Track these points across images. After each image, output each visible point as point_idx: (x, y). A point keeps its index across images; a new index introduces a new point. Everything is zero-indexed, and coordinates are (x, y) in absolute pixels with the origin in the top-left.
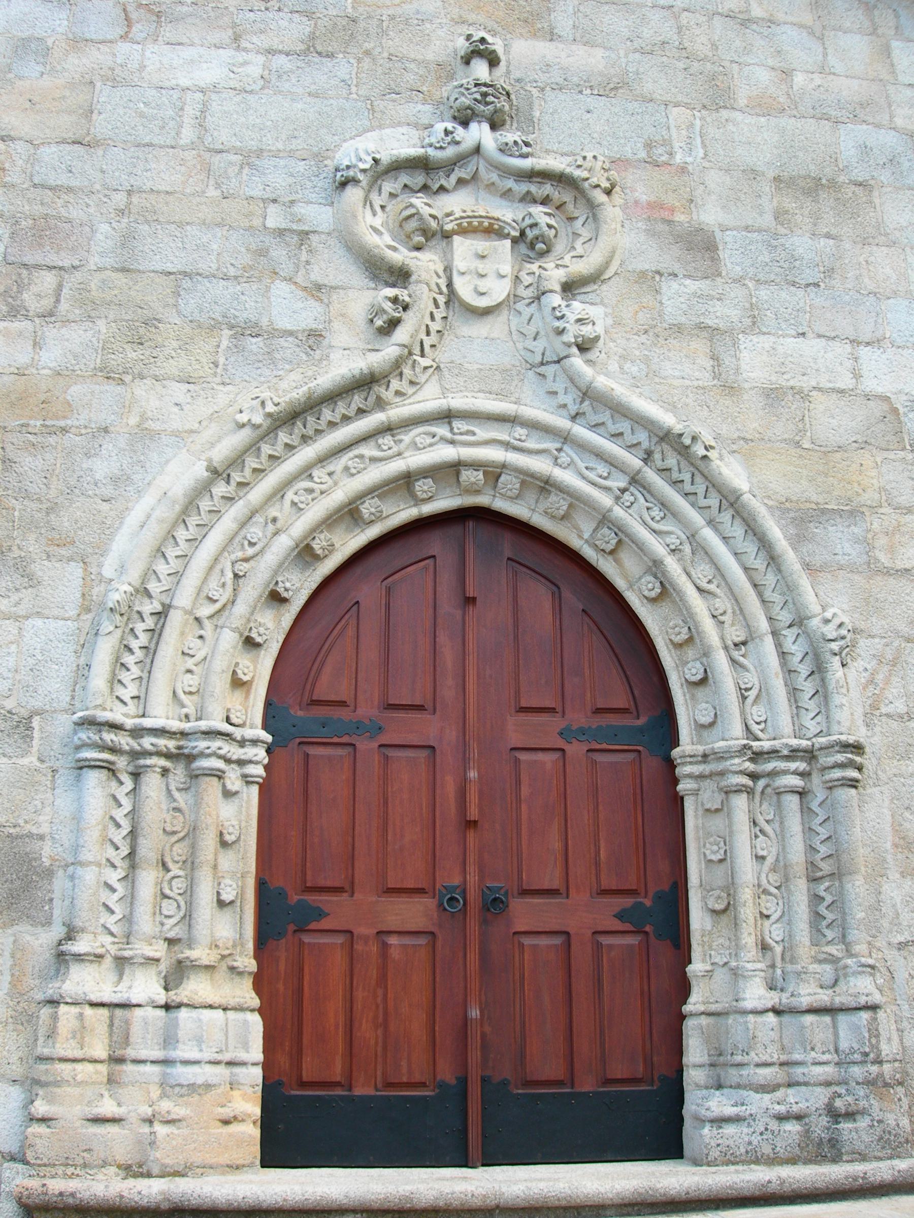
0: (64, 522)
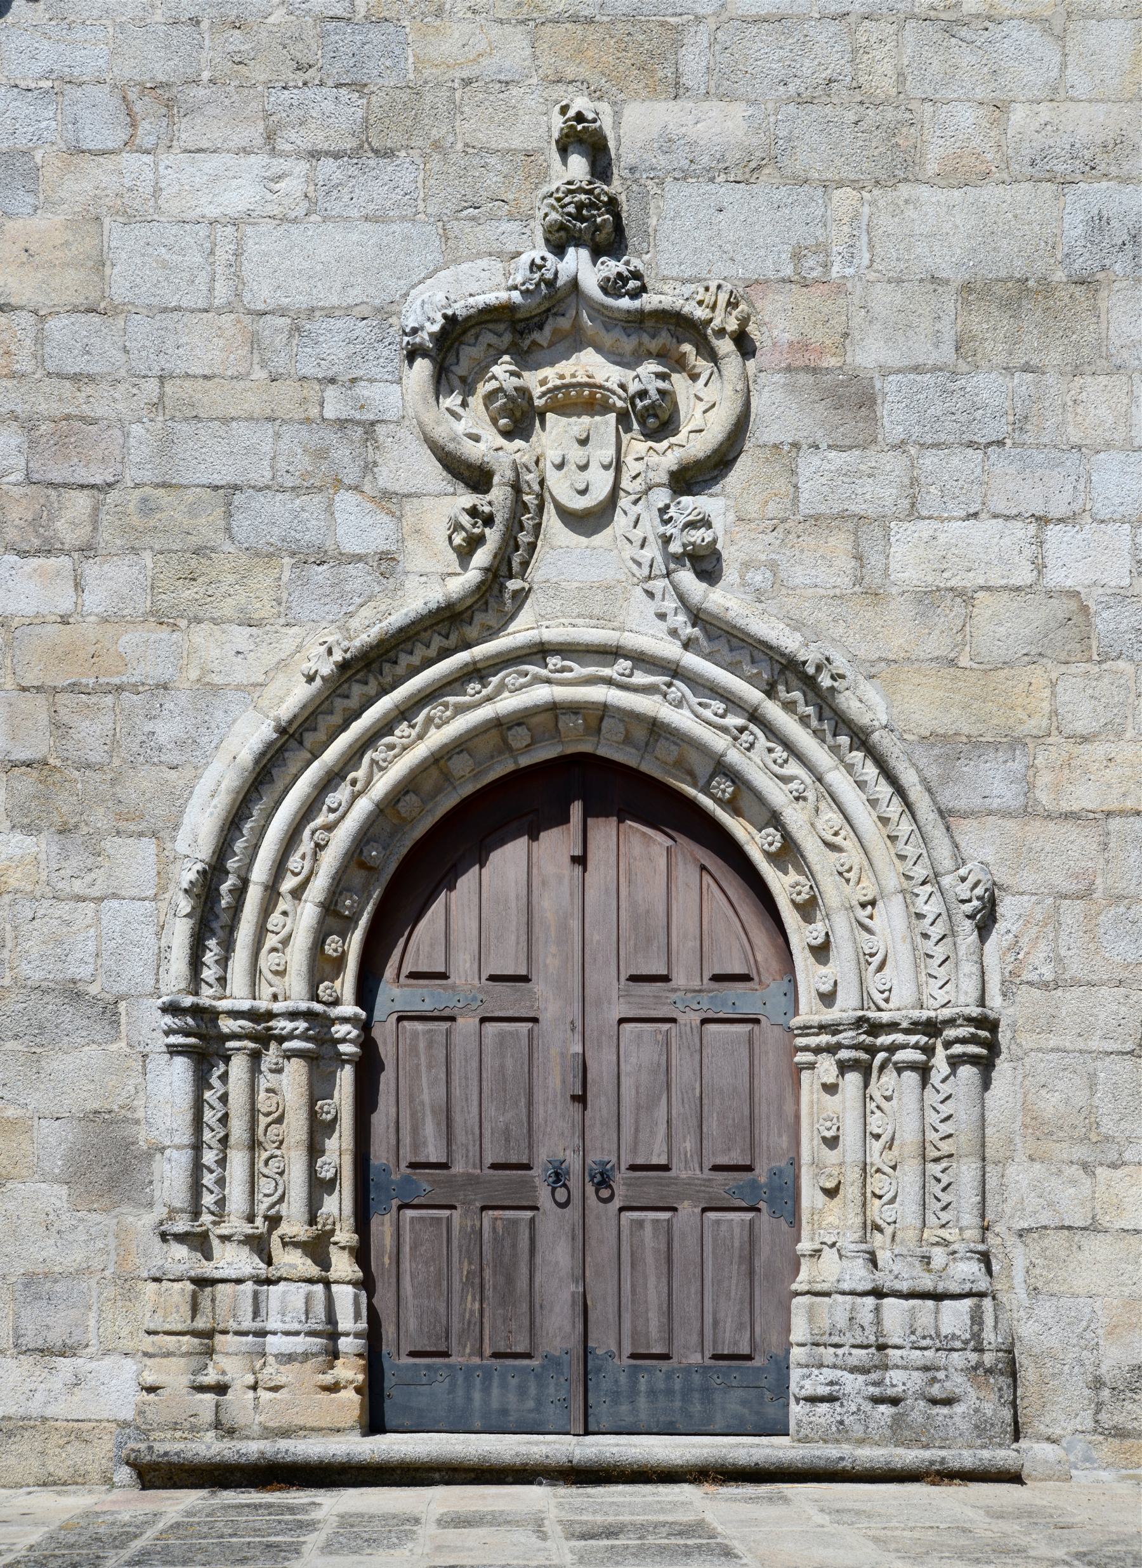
0: (129, 793)
